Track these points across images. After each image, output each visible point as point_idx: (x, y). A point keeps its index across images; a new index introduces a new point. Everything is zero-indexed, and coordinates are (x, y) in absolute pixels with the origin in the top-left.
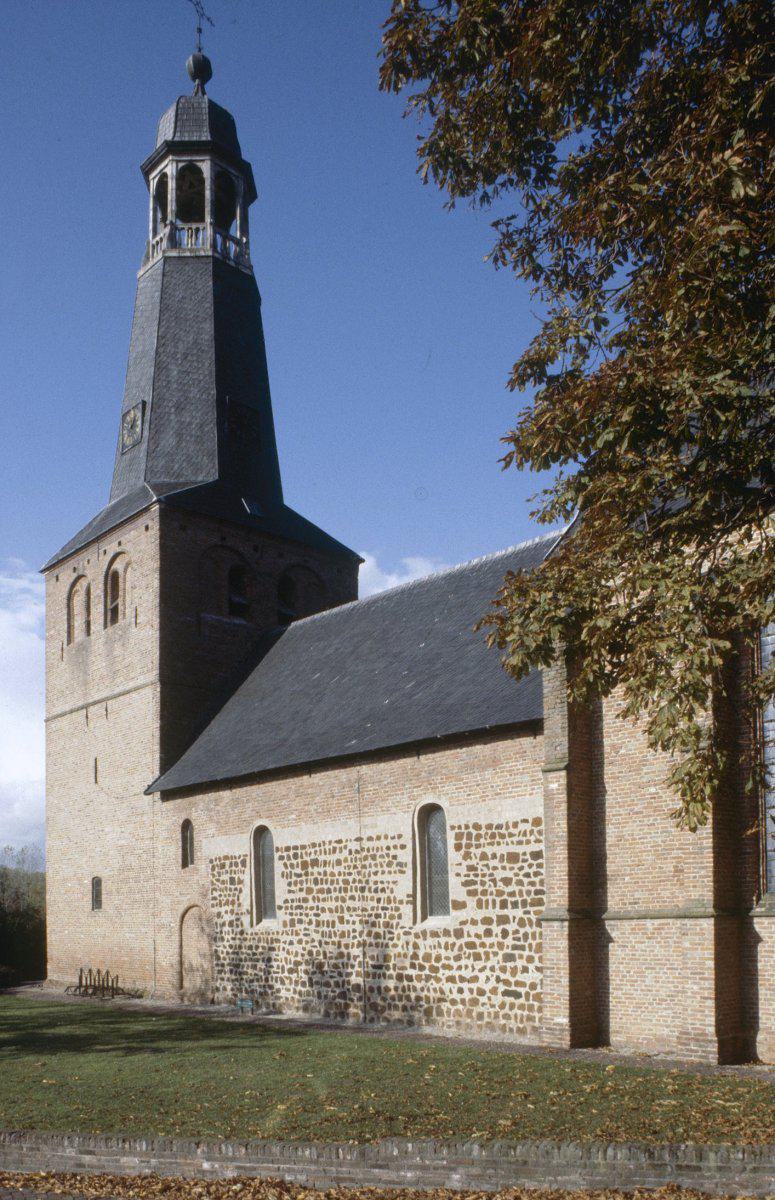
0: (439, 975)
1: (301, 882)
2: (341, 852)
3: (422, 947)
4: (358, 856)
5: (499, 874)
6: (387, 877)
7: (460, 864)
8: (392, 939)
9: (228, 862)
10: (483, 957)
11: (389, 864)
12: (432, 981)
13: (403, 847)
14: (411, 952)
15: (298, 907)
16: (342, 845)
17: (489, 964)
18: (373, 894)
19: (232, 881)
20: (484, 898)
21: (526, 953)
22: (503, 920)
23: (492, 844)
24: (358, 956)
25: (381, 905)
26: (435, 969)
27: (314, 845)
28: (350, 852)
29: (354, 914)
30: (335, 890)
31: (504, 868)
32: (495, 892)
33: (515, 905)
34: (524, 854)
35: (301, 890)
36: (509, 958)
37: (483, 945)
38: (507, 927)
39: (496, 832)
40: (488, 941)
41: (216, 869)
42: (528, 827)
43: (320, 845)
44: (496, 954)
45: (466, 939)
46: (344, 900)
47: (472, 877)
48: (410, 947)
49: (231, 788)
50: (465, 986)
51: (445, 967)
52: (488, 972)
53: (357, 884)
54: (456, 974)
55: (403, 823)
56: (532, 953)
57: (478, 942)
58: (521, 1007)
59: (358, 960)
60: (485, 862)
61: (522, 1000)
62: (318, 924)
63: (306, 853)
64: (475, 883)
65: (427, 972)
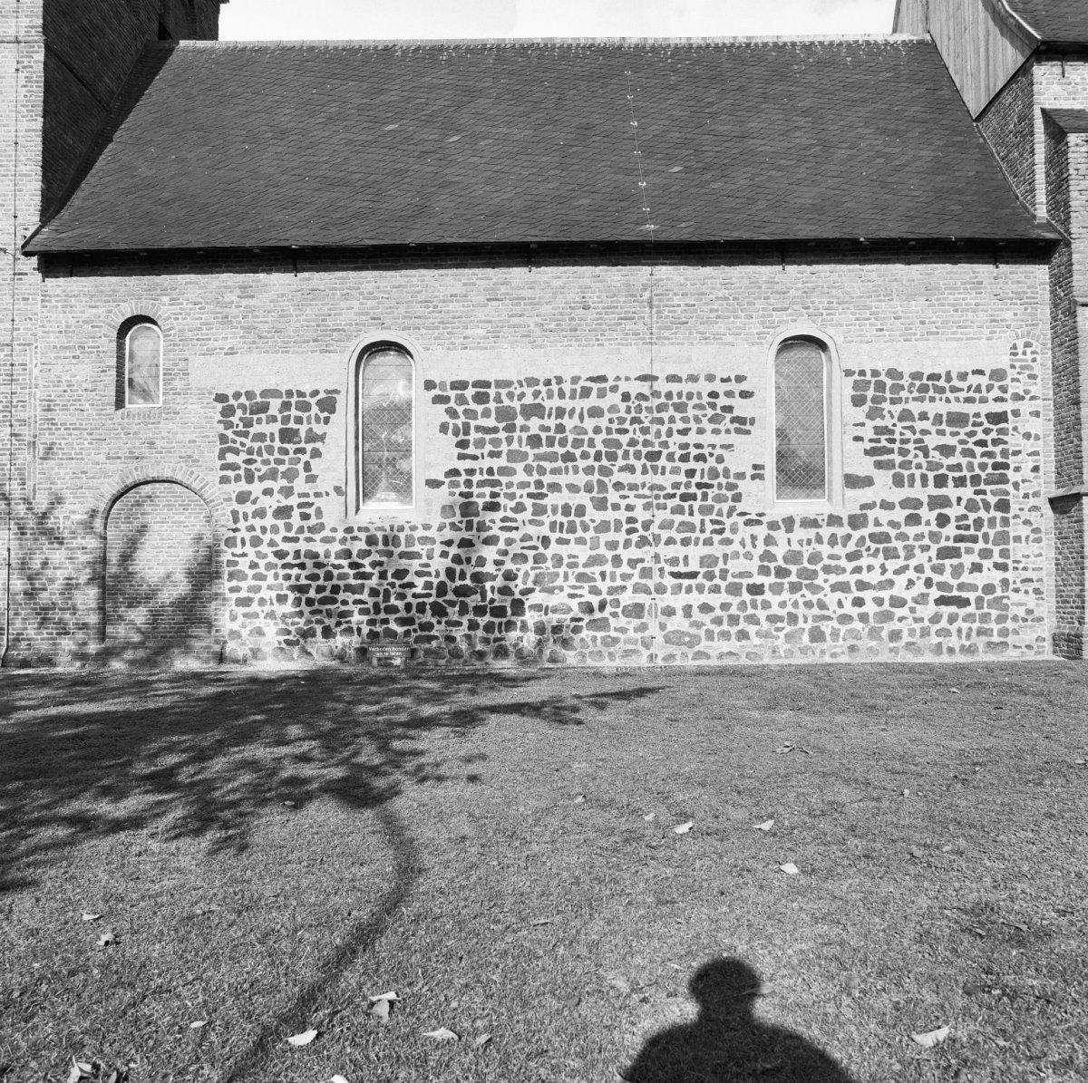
2: (602, 394)
4: (644, 404)
6: (707, 439)
7: (863, 424)
8: (721, 532)
10: (902, 553)
18: (678, 464)
20: (906, 473)
21: (981, 545)
24: (642, 561)
25: (697, 479)
28: (626, 397)
32: (925, 465)
33: (960, 482)
34: (977, 415)
38: (946, 511)
40: (911, 531)
42: (984, 381)
45: (871, 529)
46: (605, 472)
47: (884, 443)
48: (760, 543)
53: (639, 447)
56: (990, 546)
57: (893, 532)
60: (908, 424)
64: (891, 451)
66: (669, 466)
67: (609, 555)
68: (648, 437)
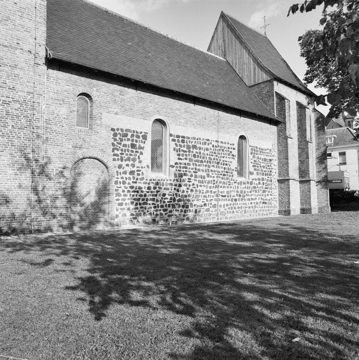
0: (245, 198)
1: (186, 155)
2: (208, 145)
3: (240, 188)
4: (217, 149)
5: (262, 165)
6: (228, 160)
8: (230, 185)
9: (130, 134)
11: (229, 155)
12: (243, 201)
13: (234, 149)
14: (236, 190)
15: (183, 167)
16: (210, 142)
17: (259, 194)
18: (222, 166)
19: (133, 146)
21: (268, 190)
22: (263, 179)
23: (260, 154)
24: (216, 192)
25: (226, 170)
26: (244, 196)
27: (194, 138)
28: (213, 146)
29: (214, 173)
30: (205, 161)
31: (263, 163)
35: (186, 159)
36: (264, 191)
37: (258, 187)
39: (262, 151)
40: (259, 186)
41: (119, 136)
43: (197, 139)
44: (261, 190)
45: (253, 185)
46: (209, 167)
48: (236, 188)
49: (136, 89)
50: (253, 201)
51: (247, 195)
52: (259, 196)
53: (215, 160)
54: (250, 197)
55: (235, 140)
57: (256, 186)
58: (267, 207)
59: (216, 193)
61: (267, 205)
62: (196, 177)
63: (189, 141)
65: (242, 197)
66: (221, 166)
67: (210, 190)
68: (217, 158)
